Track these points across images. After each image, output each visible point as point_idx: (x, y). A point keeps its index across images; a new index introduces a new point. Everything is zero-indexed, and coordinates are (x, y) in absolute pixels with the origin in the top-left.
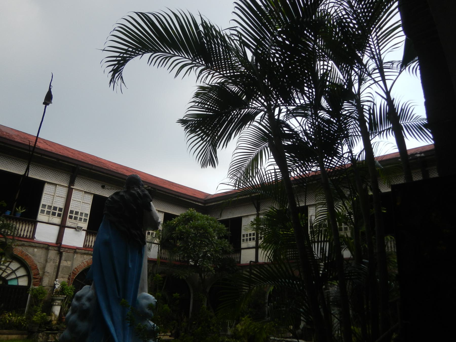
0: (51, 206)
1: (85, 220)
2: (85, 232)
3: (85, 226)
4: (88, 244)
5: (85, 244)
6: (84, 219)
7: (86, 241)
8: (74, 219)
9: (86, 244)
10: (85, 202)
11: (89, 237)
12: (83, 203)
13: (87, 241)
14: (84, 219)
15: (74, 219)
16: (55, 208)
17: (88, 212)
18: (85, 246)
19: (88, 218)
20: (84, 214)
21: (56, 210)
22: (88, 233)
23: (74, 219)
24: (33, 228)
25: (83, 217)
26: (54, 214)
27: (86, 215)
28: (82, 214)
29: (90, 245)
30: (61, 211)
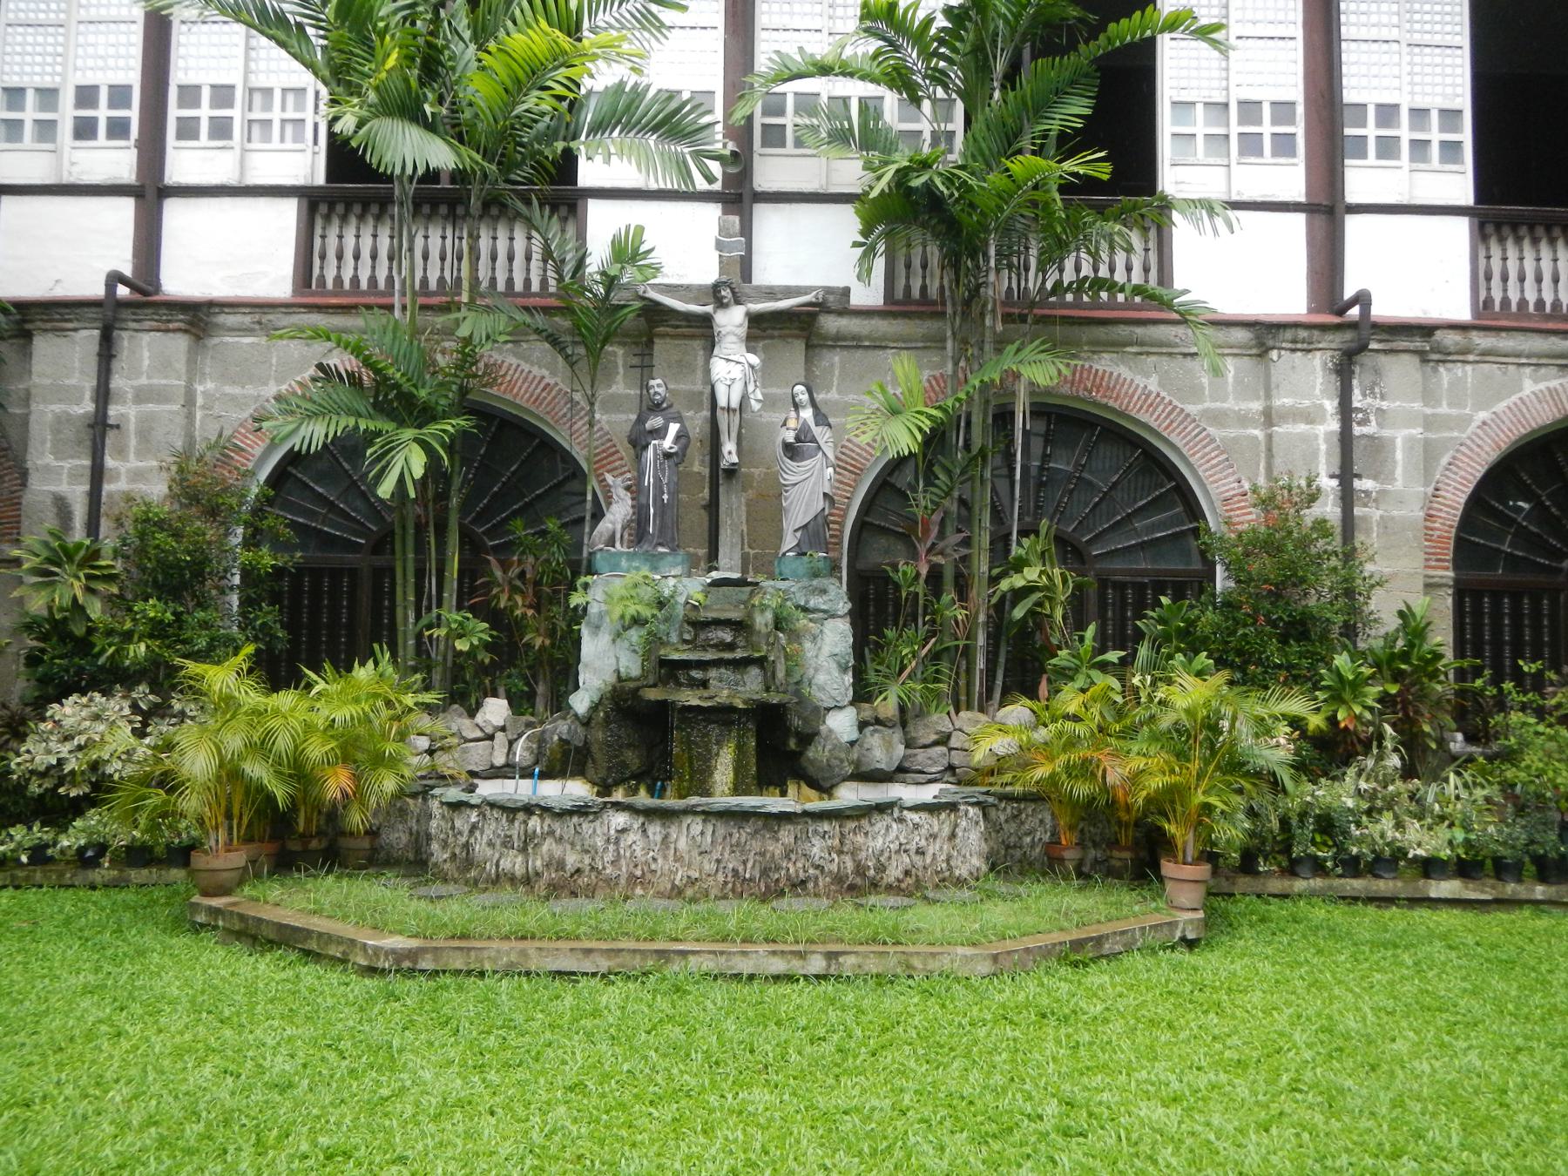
0: (1226, 105)
1: (1450, 150)
2: (1461, 228)
3: (1460, 186)
4: (1497, 296)
5: (1483, 295)
6: (1443, 144)
7: (1480, 277)
8: (1380, 156)
9: (1488, 302)
10: (1427, 38)
11: (1496, 251)
12: (1417, 50)
13: (1488, 278)
14: (1443, 144)
15: (1380, 156)
16: (1250, 110)
17: (1463, 100)
18: (1483, 306)
19: (1466, 136)
20: (1435, 115)
21: (1259, 122)
22: (1490, 229)
23: (1381, 155)
24: (1152, 245)
25: (1435, 136)
26: (1251, 145)
27: (1450, 117)
28: (1420, 114)
29: (1514, 297)
30: (1292, 122)
